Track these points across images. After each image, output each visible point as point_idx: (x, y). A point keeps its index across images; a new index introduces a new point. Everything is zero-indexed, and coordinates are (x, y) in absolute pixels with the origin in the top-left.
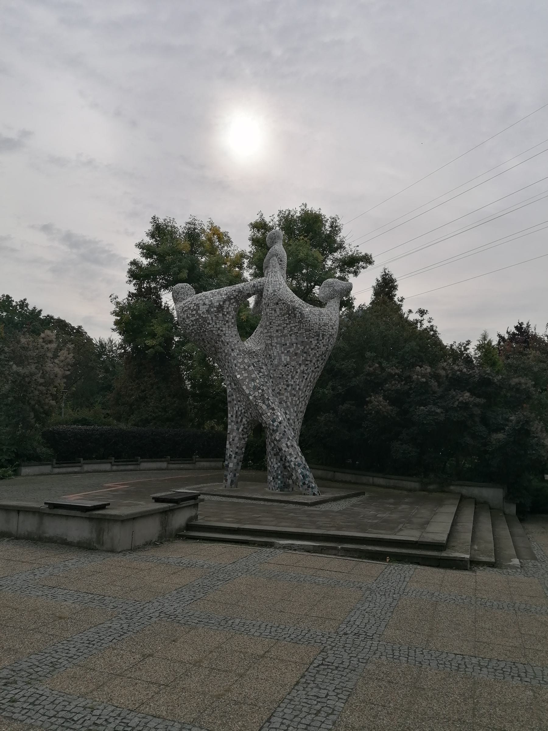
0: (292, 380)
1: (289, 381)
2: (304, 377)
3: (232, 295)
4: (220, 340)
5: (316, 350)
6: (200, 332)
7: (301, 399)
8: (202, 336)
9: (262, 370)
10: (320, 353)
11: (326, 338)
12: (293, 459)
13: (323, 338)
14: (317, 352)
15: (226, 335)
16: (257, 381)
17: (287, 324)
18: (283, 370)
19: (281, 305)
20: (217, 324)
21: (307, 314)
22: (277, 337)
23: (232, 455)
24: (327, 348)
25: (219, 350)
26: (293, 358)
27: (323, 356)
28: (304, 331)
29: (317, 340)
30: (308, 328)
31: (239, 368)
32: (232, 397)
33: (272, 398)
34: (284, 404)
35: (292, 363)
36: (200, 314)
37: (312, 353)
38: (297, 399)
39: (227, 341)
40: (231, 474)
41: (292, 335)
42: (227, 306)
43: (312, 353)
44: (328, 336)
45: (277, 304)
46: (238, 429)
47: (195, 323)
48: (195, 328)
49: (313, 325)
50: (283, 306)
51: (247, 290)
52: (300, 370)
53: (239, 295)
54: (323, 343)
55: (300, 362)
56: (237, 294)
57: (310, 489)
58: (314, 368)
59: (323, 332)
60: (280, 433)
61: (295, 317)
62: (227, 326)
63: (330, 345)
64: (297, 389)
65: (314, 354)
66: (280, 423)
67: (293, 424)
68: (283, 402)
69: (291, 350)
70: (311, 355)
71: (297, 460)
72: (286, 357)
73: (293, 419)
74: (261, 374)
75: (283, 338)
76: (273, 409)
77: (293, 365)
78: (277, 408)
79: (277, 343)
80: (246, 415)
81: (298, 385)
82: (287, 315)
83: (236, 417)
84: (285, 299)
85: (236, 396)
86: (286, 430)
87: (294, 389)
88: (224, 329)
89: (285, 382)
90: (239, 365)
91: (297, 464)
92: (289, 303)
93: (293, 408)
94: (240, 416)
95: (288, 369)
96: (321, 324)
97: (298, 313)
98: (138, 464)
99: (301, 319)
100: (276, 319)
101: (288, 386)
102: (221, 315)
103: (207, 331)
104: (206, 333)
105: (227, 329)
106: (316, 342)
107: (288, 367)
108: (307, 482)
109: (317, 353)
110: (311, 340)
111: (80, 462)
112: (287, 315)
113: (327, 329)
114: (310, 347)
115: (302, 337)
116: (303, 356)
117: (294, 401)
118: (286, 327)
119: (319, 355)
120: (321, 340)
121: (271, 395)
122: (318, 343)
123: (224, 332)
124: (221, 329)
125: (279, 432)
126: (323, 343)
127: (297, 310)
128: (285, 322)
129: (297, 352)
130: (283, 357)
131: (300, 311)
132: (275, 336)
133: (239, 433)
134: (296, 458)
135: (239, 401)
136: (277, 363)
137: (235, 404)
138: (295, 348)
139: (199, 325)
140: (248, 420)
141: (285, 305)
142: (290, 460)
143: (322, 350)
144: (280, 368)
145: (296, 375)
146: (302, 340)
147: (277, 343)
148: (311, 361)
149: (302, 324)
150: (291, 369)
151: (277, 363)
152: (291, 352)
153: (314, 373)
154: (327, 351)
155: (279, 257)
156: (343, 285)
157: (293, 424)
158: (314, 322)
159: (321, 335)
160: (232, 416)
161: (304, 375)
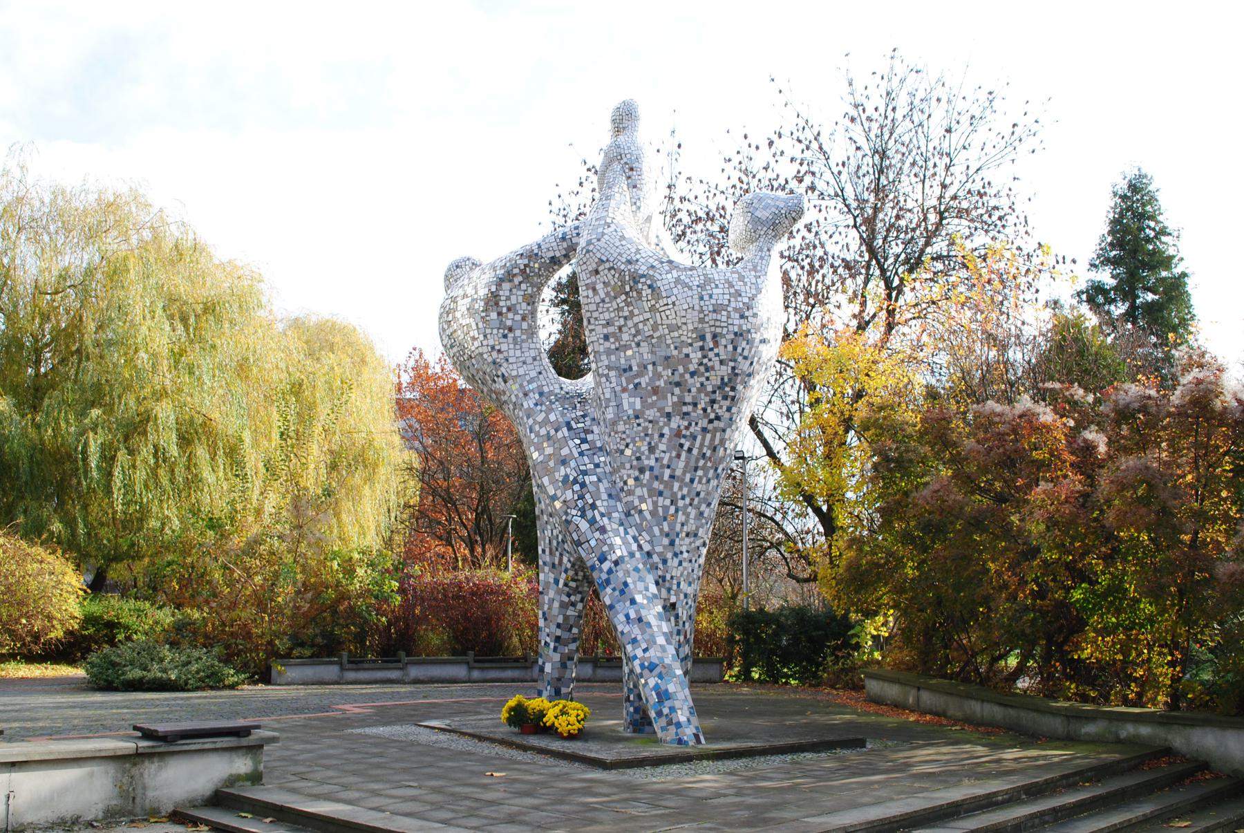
0: (652, 456)
1: (643, 457)
2: (681, 446)
3: (516, 266)
4: (499, 373)
5: (702, 375)
7: (681, 503)
9: (590, 437)
10: (714, 382)
11: (723, 342)
12: (639, 653)
13: (716, 344)
14: (708, 379)
15: (511, 360)
16: (573, 464)
17: (625, 318)
18: (627, 432)
19: (605, 275)
20: (489, 336)
21: (667, 287)
22: (609, 352)
24: (733, 368)
26: (649, 400)
27: (727, 389)
28: (666, 331)
29: (702, 348)
30: (674, 322)
31: (538, 435)
33: (605, 503)
34: (636, 516)
35: (647, 412)
37: (694, 382)
38: (668, 502)
39: (514, 373)
40: (549, 688)
41: (642, 344)
42: (507, 293)
43: (694, 382)
44: (732, 336)
45: (597, 272)
46: (557, 582)
49: (683, 313)
50: (609, 275)
51: (548, 249)
52: (671, 429)
53: (532, 264)
54: (717, 355)
55: (669, 409)
56: (526, 261)
57: (672, 729)
58: (706, 421)
59: (713, 329)
60: (614, 589)
61: (640, 299)
62: (510, 339)
63: (740, 359)
64: (666, 477)
65: (698, 385)
66: (616, 563)
67: (660, 566)
68: (633, 512)
69: (644, 381)
70: (694, 390)
71: (647, 655)
72: (632, 400)
73: (659, 554)
74: (585, 446)
75: (622, 354)
76: (603, 530)
77: (650, 418)
78: (615, 526)
79: (609, 368)
81: (668, 467)
82: (623, 297)
83: (551, 553)
84: (611, 259)
86: (629, 580)
87: (657, 478)
88: (504, 347)
89: (635, 463)
90: (537, 428)
91: (646, 664)
92: (622, 267)
93: (659, 524)
95: (640, 428)
96: (705, 308)
97: (646, 287)
98: (526, 668)
99: (653, 302)
100: (600, 310)
101: (642, 471)
102: (494, 315)
105: (512, 346)
106: (699, 354)
107: (639, 425)
108: (666, 711)
109: (706, 383)
110: (685, 351)
111: (399, 661)
112: (623, 297)
113: (724, 319)
114: (686, 369)
115: (663, 345)
116: (673, 394)
117: (660, 510)
118: (625, 325)
119: (713, 386)
120: (711, 349)
121: (605, 496)
122: (704, 357)
123: (505, 354)
124: (497, 347)
125: (612, 586)
126: (717, 355)
127: (643, 280)
128: (621, 314)
129: (657, 383)
130: (626, 400)
131: (649, 282)
132: (602, 350)
133: (559, 592)
134: (645, 650)
136: (612, 416)
138: (651, 374)
140: (572, 559)
141: (613, 272)
142: (631, 655)
143: (719, 373)
144: (621, 427)
145: (660, 441)
146: (663, 354)
147: (609, 368)
148: (695, 405)
149: (658, 314)
150: (646, 429)
151: (612, 416)
152: (644, 385)
153: (709, 436)
154: (737, 375)
155: (625, 160)
156: (777, 203)
157: (660, 566)
158: (686, 306)
159: (709, 337)
160: (544, 551)
161: (683, 441)
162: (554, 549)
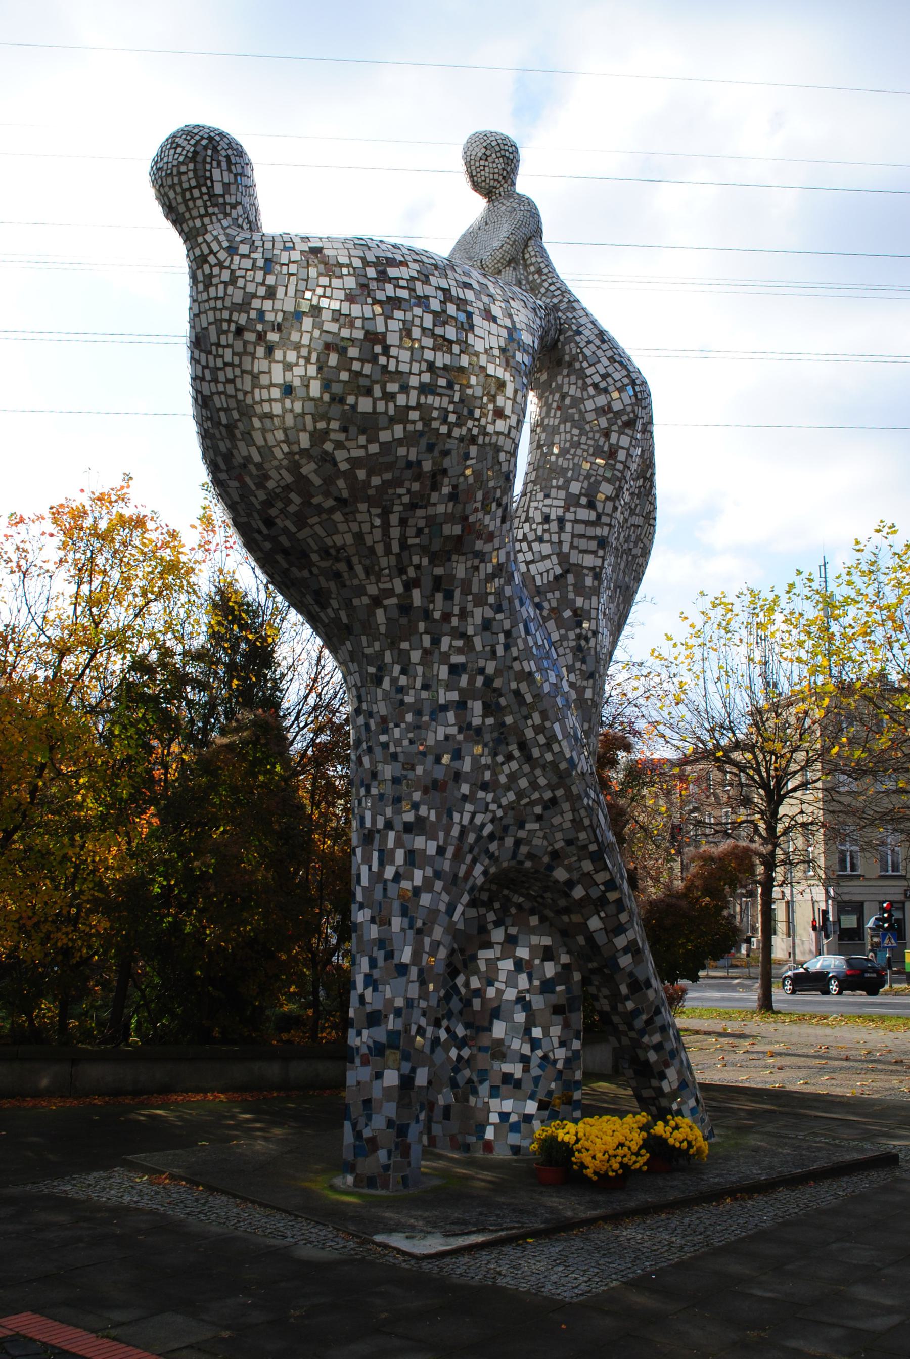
6: (449, 435)
8: (446, 453)
23: (424, 1031)
25: (479, 545)
32: (456, 765)
36: (477, 354)
47: (442, 382)
48: (432, 407)
80: (493, 847)
85: (475, 760)
94: (471, 851)
103: (480, 440)
104: (473, 451)
135: (485, 787)
137: (465, 798)
139: (462, 401)
162: (466, 848)
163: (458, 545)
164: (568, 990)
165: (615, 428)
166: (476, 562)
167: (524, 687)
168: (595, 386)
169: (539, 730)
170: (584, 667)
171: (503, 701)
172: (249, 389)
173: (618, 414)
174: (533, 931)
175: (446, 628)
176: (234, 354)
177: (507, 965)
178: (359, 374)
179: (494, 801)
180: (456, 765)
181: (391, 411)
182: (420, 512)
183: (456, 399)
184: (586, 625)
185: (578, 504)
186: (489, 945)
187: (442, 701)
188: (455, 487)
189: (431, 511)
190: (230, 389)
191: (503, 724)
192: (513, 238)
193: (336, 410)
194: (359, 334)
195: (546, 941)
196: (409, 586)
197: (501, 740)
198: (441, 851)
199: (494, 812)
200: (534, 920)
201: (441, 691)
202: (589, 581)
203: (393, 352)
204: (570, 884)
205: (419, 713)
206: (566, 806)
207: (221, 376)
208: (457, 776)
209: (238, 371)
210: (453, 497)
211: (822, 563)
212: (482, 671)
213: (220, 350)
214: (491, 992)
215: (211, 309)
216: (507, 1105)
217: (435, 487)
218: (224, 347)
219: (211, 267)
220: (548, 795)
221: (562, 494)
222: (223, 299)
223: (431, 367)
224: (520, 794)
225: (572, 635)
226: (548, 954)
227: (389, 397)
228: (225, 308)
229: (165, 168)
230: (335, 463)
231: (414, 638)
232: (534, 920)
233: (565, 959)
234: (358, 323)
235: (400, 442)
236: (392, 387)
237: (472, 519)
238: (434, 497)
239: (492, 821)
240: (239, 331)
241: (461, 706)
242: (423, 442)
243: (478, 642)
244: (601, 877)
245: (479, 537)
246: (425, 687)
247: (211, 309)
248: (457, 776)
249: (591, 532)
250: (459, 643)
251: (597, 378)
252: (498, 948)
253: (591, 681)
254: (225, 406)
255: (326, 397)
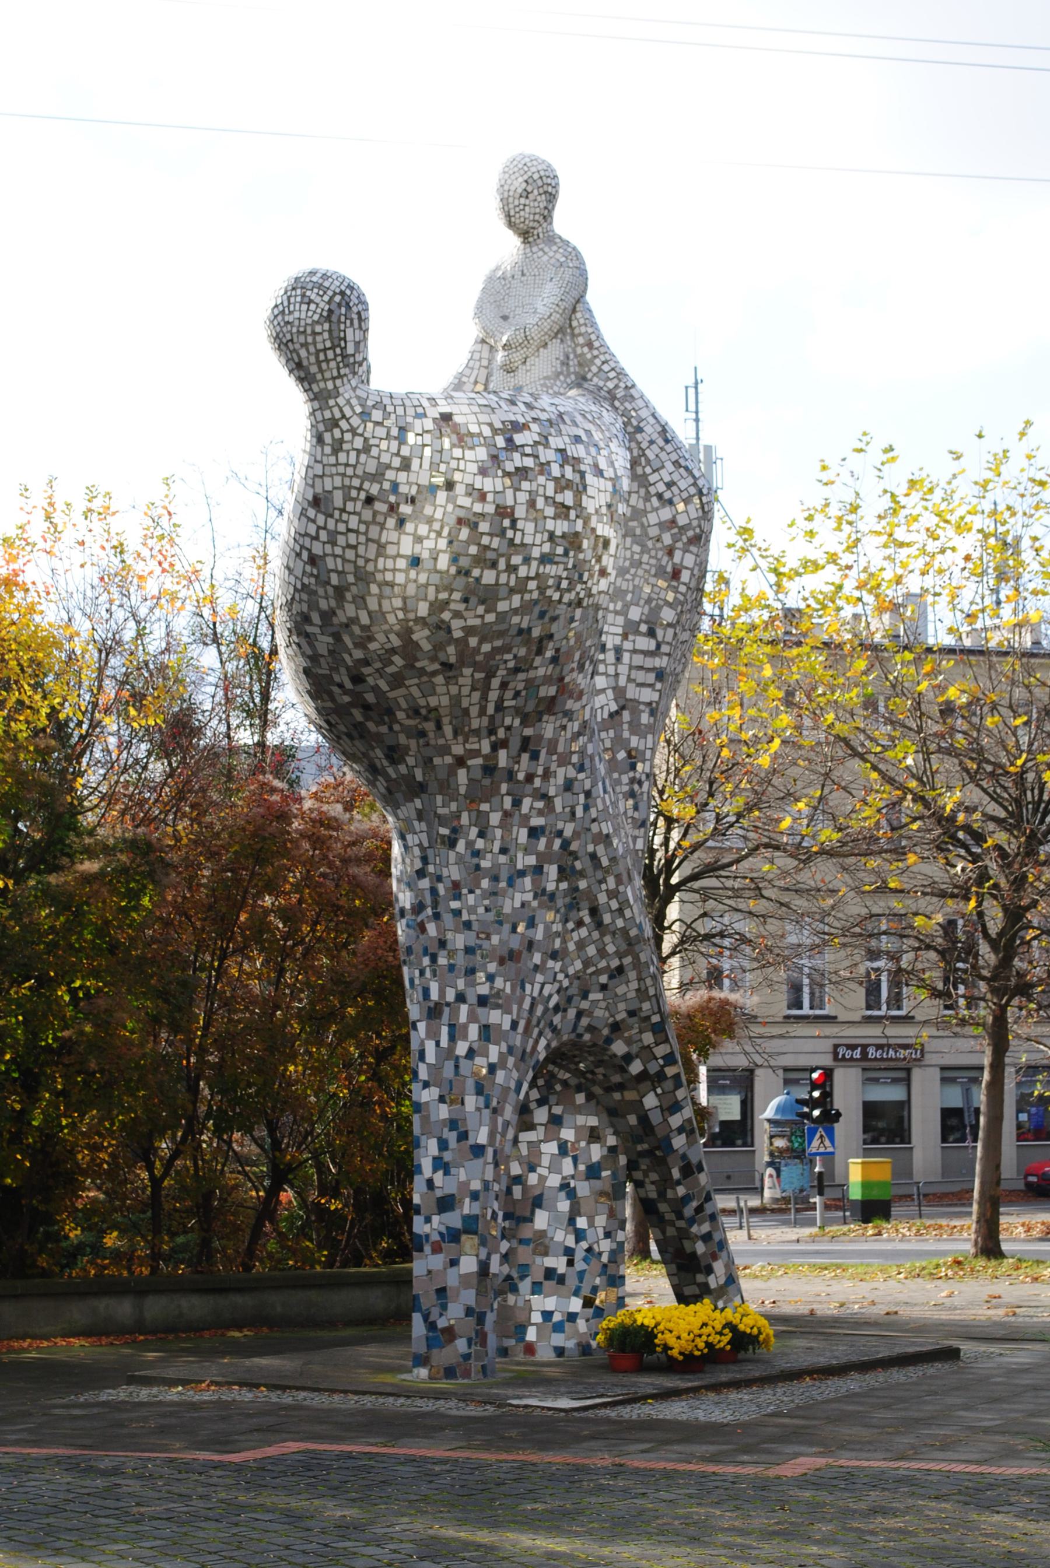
8: (554, 619)
25: (570, 704)
32: (530, 933)
47: (560, 550)
80: (557, 1019)
135: (554, 955)
137: (536, 968)
162: (534, 1022)
163: (550, 706)
164: (614, 1175)
165: (679, 545)
166: (565, 721)
167: (601, 850)
168: (660, 496)
169: (612, 894)
170: (636, 815)
171: (578, 865)
172: (372, 557)
173: (683, 529)
174: (579, 1110)
175: (528, 789)
176: (360, 522)
177: (551, 1148)
178: (487, 548)
179: (561, 971)
180: (530, 933)
181: (512, 583)
182: (521, 676)
183: (570, 566)
184: (640, 767)
185: (637, 632)
186: (531, 1127)
187: (520, 866)
188: (557, 650)
189: (532, 674)
190: (350, 554)
191: (577, 889)
192: (563, 305)
193: (460, 582)
194: (490, 509)
195: (593, 1121)
196: (495, 747)
197: (573, 906)
198: (514, 1025)
199: (560, 982)
200: (580, 1098)
201: (520, 855)
202: (645, 718)
203: (520, 525)
204: (628, 1058)
205: (496, 879)
206: (632, 975)
207: (341, 540)
208: (531, 945)
209: (362, 539)
210: (555, 660)
211: (691, 382)
212: (560, 834)
213: (345, 517)
214: (533, 1179)
215: (338, 474)
216: (550, 1303)
217: (540, 652)
218: (350, 513)
219: (343, 432)
220: (615, 963)
221: (620, 620)
222: (355, 467)
223: (552, 536)
224: (587, 963)
225: (625, 779)
226: (594, 1135)
227: (512, 569)
228: (355, 475)
229: (296, 323)
230: (449, 631)
231: (496, 800)
232: (580, 1098)
233: (612, 1140)
234: (490, 497)
235: (515, 611)
236: (516, 560)
237: (567, 680)
238: (538, 661)
239: (558, 992)
240: (369, 500)
241: (538, 870)
242: (537, 610)
243: (558, 803)
244: (661, 1051)
245: (571, 697)
246: (504, 851)
247: (338, 474)
248: (531, 945)
249: (649, 662)
250: (540, 805)
251: (661, 487)
252: (541, 1130)
253: (642, 830)
254: (340, 568)
255: (453, 570)
